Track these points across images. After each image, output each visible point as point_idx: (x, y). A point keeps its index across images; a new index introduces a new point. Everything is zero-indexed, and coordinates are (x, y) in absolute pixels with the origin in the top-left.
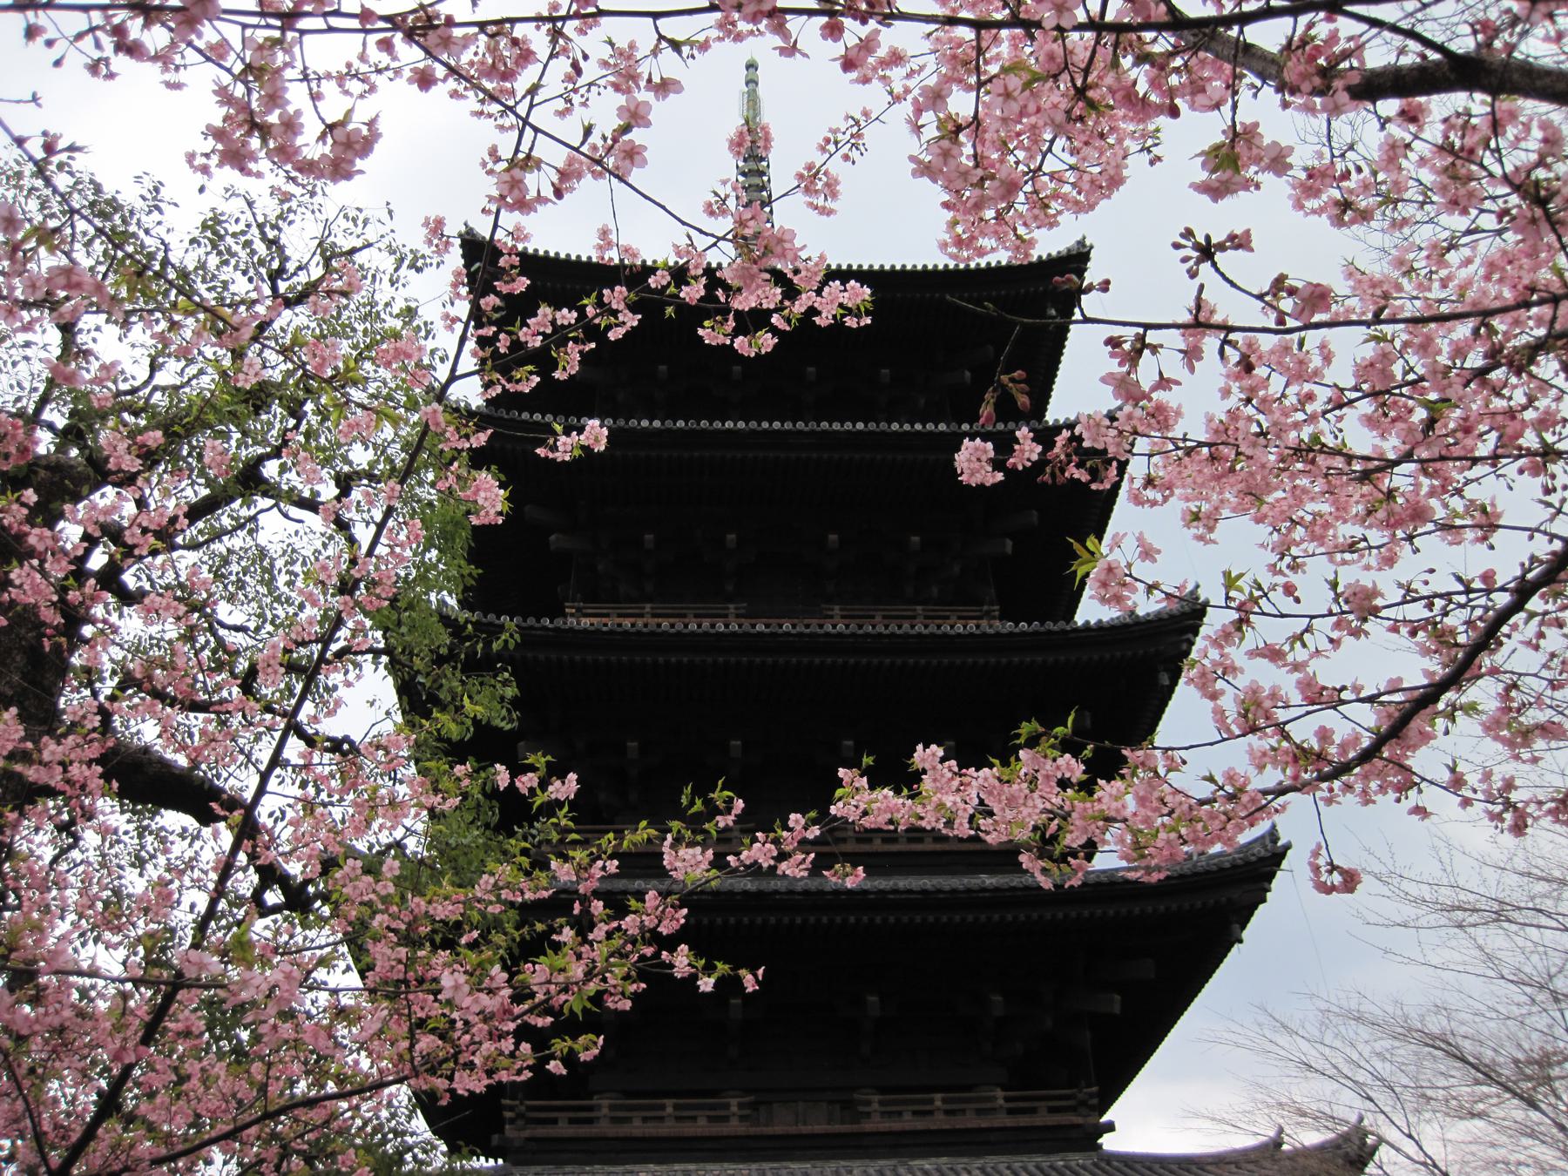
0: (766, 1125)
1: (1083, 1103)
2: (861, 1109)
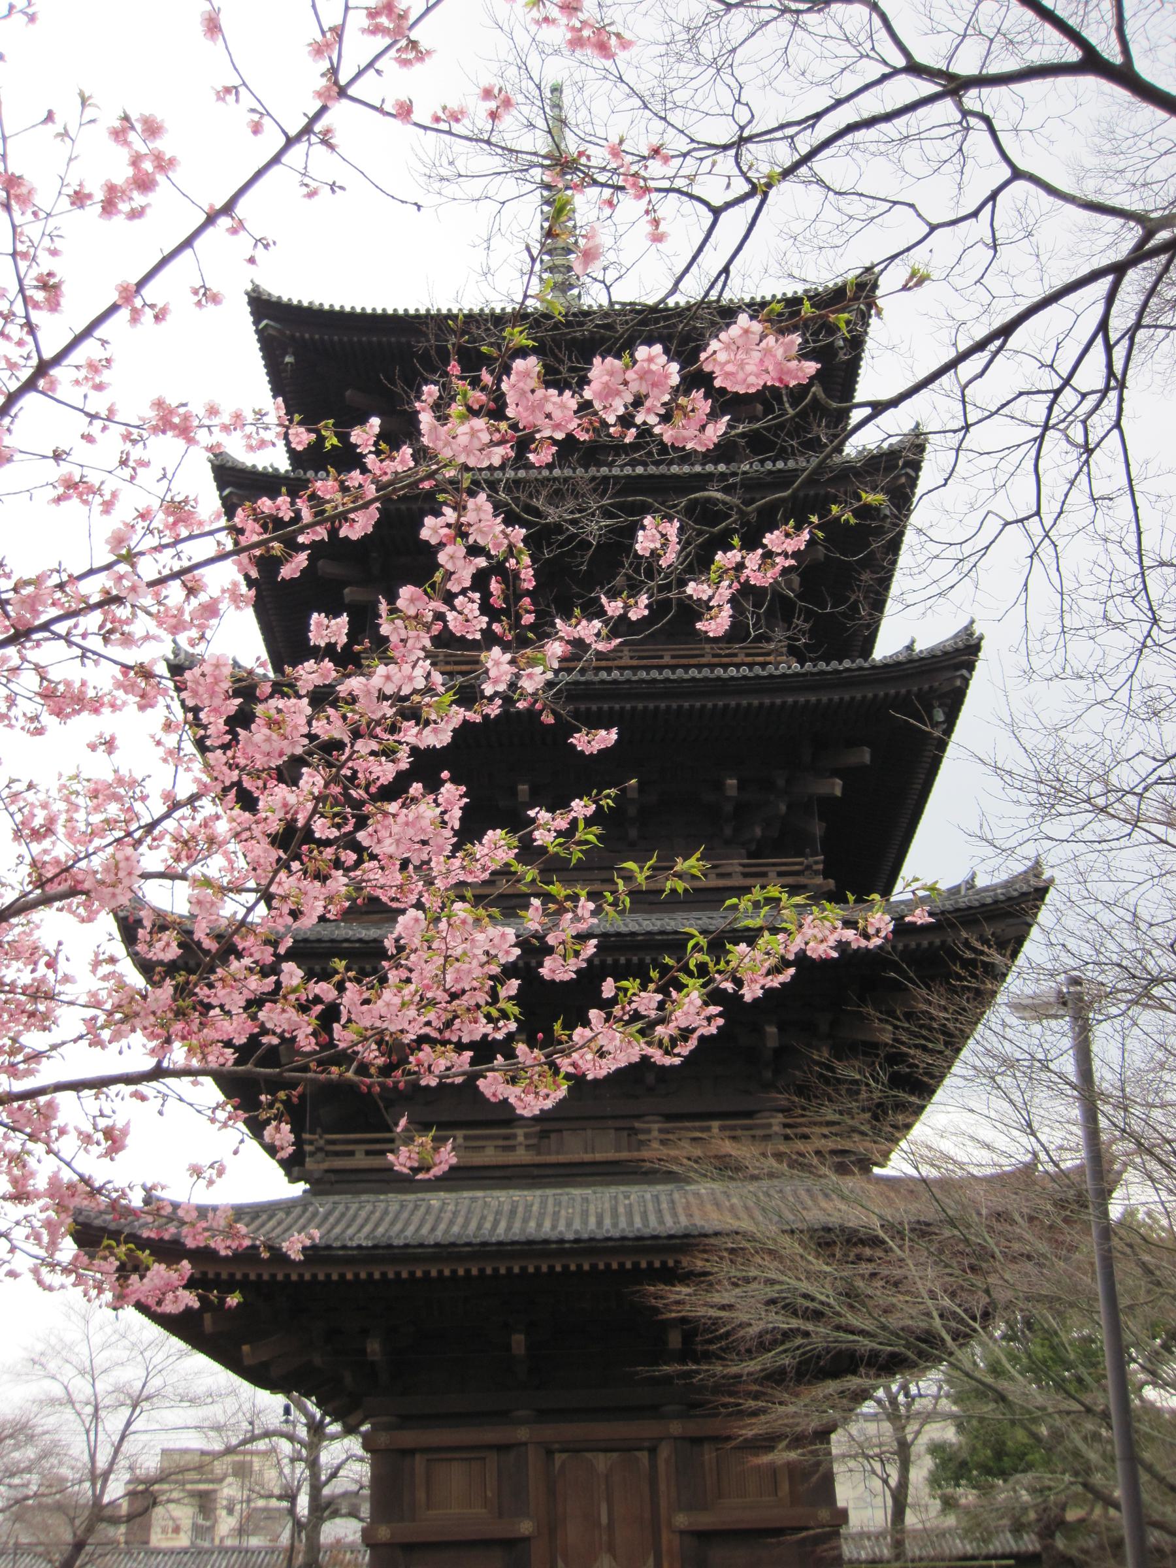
0: (558, 1153)
1: (854, 1130)
2: (642, 1137)
